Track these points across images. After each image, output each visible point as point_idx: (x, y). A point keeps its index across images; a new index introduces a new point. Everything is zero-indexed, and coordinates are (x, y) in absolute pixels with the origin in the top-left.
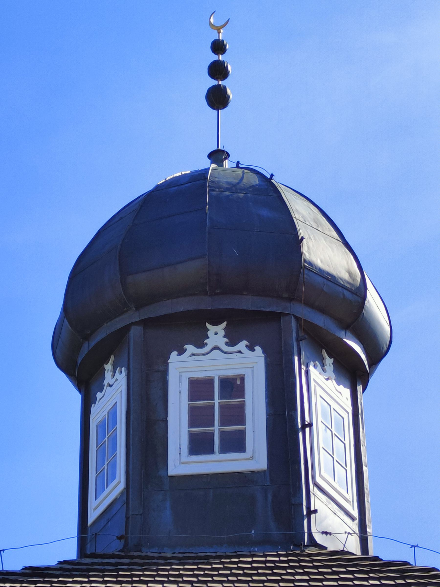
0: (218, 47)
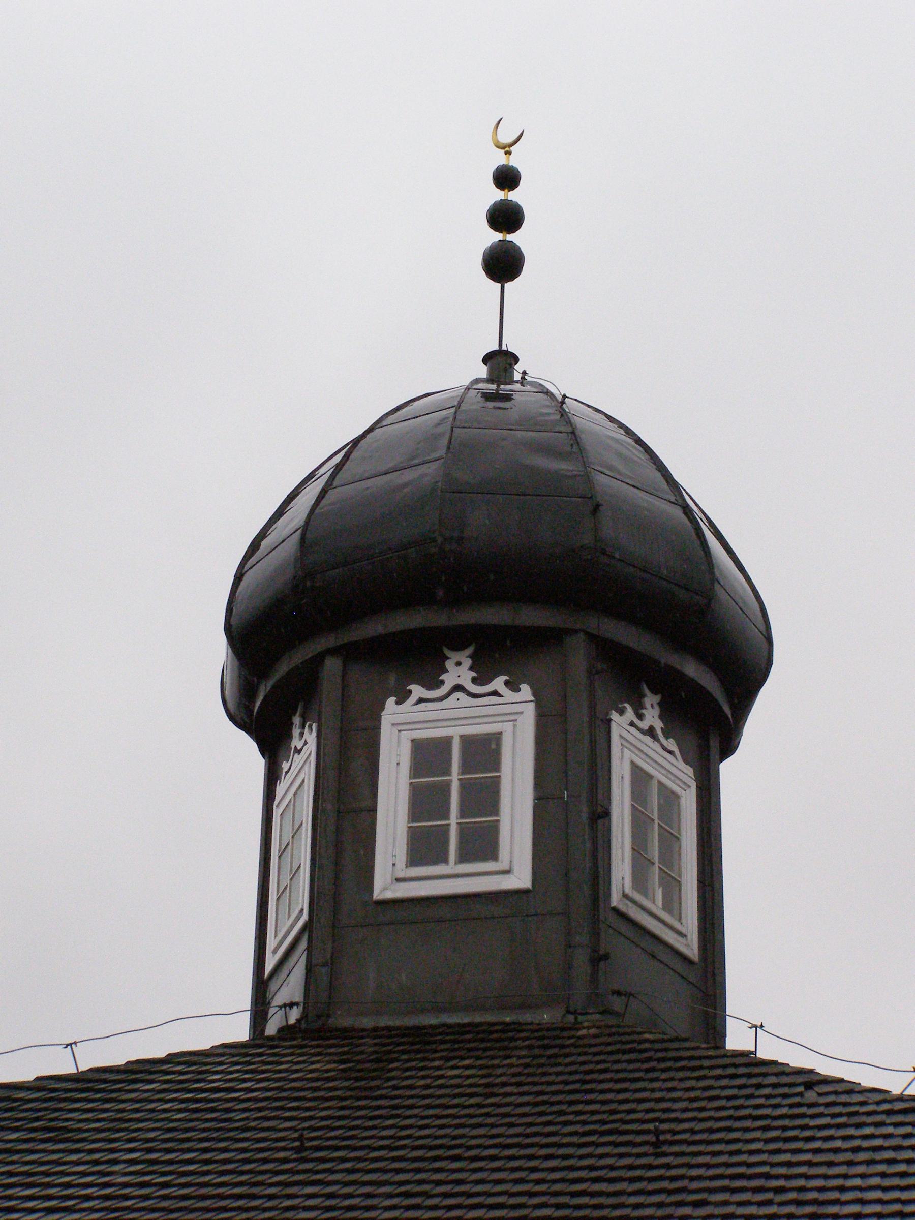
0: (507, 178)
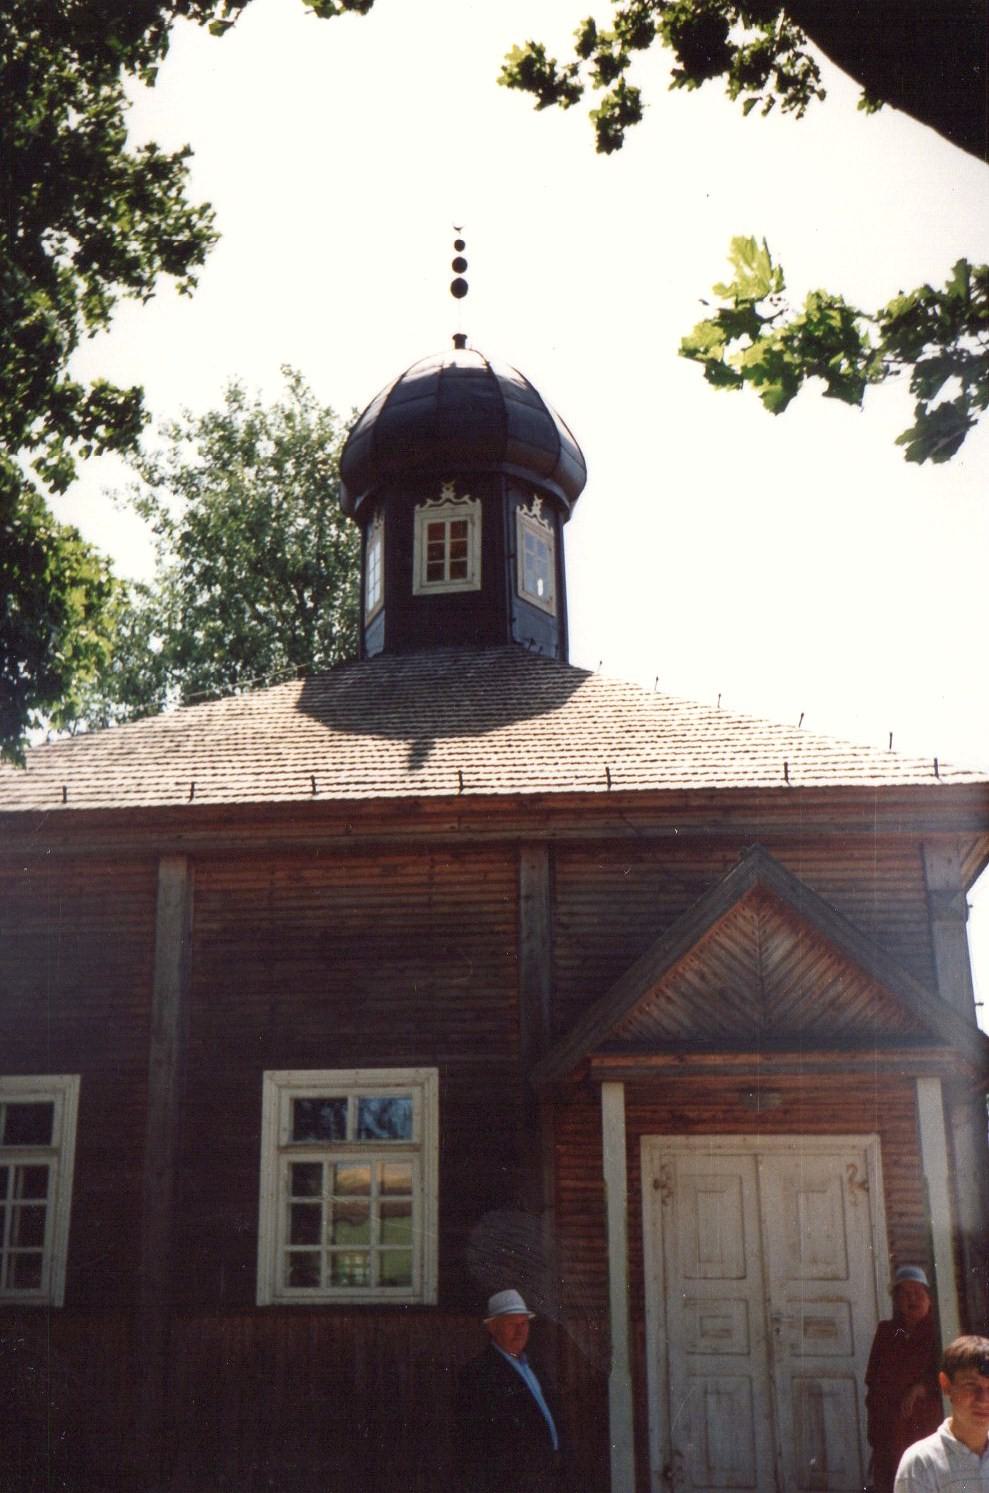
0: (460, 245)
